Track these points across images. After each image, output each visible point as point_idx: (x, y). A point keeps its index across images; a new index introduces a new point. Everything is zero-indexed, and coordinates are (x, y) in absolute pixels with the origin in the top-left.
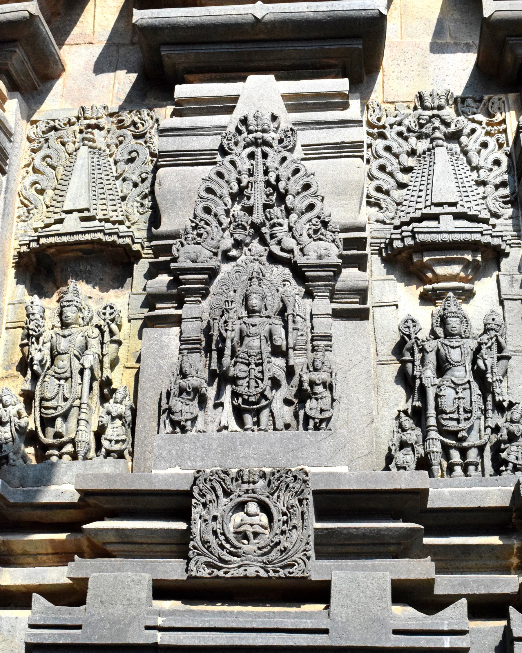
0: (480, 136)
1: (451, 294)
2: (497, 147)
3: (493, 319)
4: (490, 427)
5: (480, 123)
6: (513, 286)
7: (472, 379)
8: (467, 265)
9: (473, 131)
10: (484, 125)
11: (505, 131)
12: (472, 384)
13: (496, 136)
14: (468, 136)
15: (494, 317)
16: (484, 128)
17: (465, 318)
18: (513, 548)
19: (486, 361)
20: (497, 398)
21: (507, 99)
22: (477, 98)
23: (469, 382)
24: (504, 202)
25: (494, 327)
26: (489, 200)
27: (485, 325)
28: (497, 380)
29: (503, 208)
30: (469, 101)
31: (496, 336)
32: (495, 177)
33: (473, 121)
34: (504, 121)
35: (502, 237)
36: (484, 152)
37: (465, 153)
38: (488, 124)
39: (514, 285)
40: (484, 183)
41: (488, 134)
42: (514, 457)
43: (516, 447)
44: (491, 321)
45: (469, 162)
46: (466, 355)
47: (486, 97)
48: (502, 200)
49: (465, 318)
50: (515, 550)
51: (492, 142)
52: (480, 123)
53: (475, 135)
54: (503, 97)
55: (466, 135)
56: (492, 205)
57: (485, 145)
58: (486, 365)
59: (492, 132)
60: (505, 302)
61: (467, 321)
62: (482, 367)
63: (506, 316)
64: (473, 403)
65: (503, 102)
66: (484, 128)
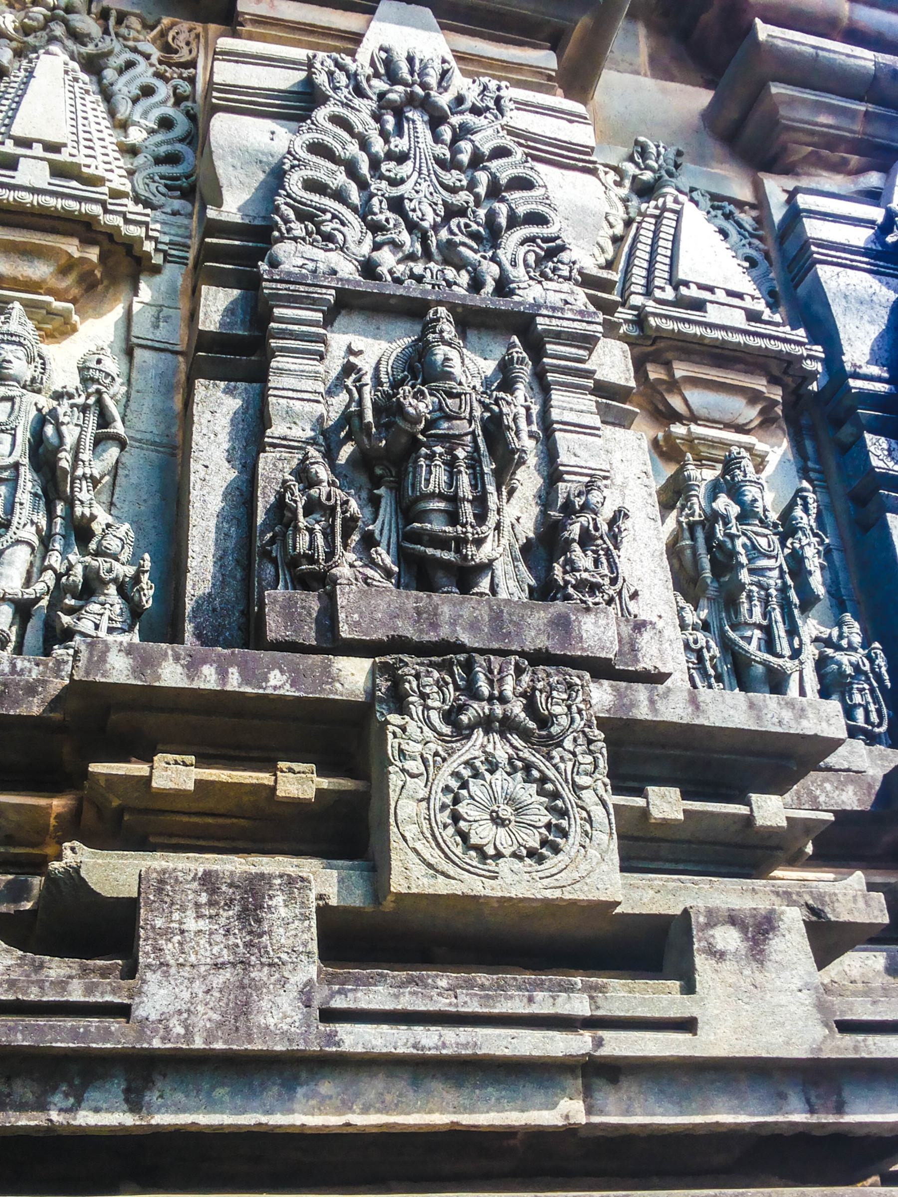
0: (143, 73)
1: (17, 305)
2: (172, 100)
3: (99, 362)
4: (55, 571)
5: (147, 57)
6: (158, 327)
7: (26, 461)
8: (67, 267)
9: (130, 65)
10: (154, 60)
11: (192, 80)
12: (22, 470)
13: (174, 82)
14: (121, 71)
15: (101, 357)
16: (152, 65)
17: (41, 357)
18: (49, 814)
19: (64, 428)
20: (78, 510)
21: (206, 31)
22: (151, 22)
23: (16, 466)
24: (166, 186)
25: (97, 375)
26: (139, 178)
27: (81, 370)
28: (84, 475)
29: (163, 195)
30: (135, 22)
31: (98, 392)
32: (158, 145)
33: (135, 50)
34: (193, 64)
35: (146, 224)
36: (145, 103)
37: (107, 95)
38: (161, 62)
39: (161, 324)
40: (132, 151)
41: (158, 75)
42: (92, 625)
43: (99, 606)
44: (93, 364)
45: (112, 113)
46: (22, 414)
47: (166, 21)
48: (163, 181)
49: (41, 357)
50: (53, 822)
51: (163, 91)
52: (147, 57)
53: (132, 72)
54: (199, 28)
55: (115, 69)
56: (142, 186)
57: (148, 91)
58: (60, 436)
59: (168, 74)
60: (138, 353)
61: (44, 364)
62: (54, 440)
63: (134, 375)
64: (17, 506)
65: (198, 36)
66: (152, 65)
